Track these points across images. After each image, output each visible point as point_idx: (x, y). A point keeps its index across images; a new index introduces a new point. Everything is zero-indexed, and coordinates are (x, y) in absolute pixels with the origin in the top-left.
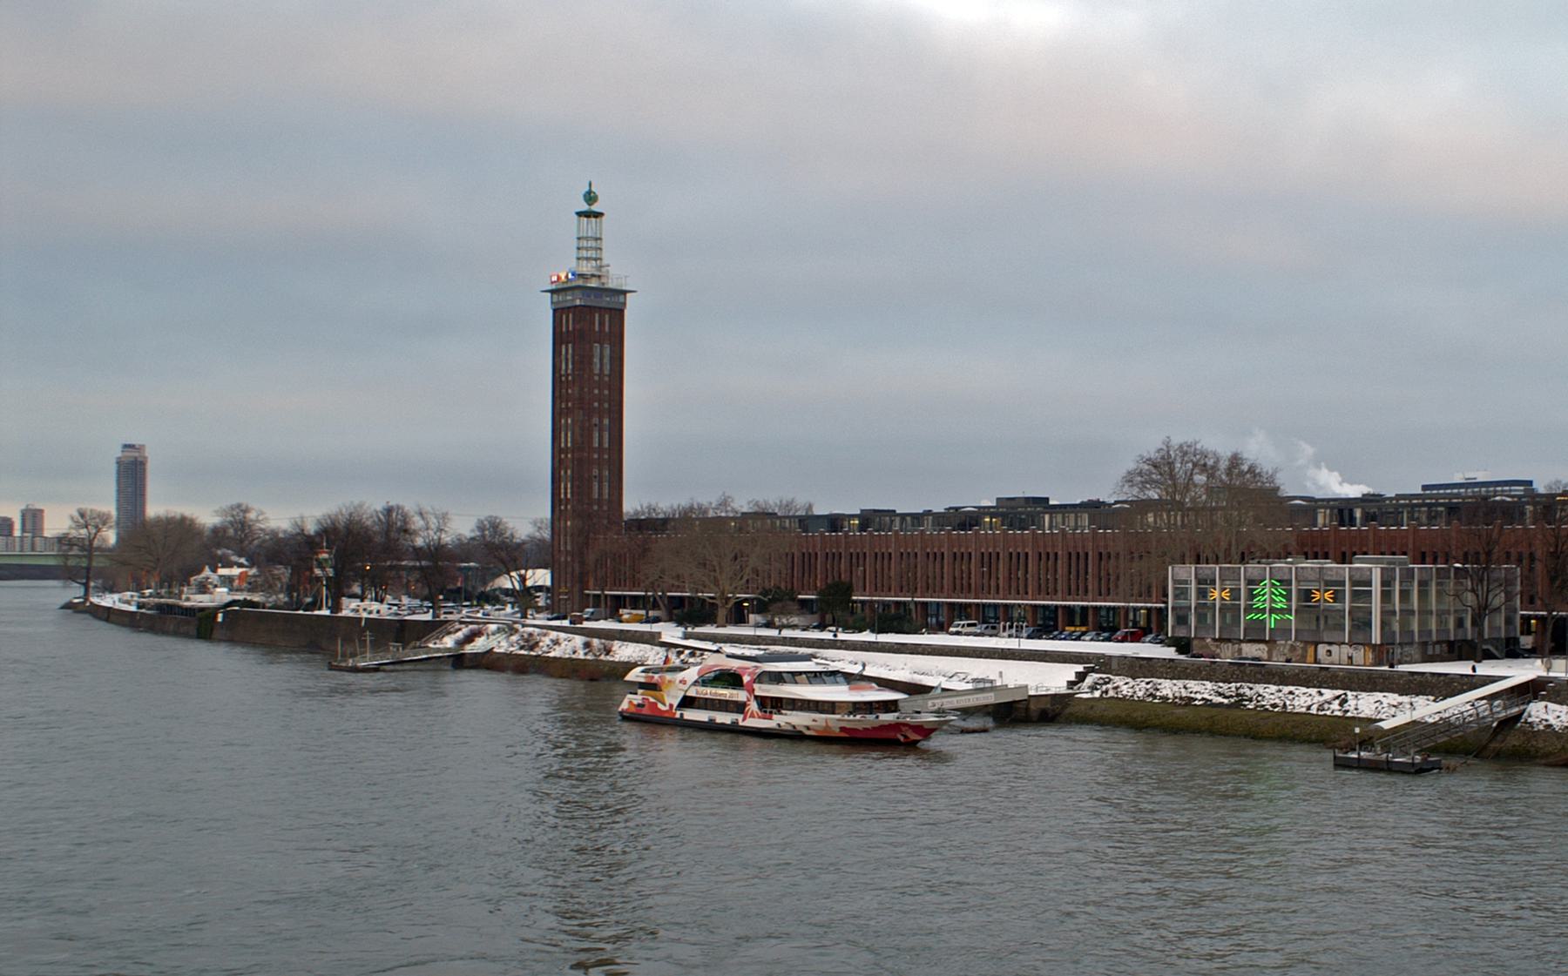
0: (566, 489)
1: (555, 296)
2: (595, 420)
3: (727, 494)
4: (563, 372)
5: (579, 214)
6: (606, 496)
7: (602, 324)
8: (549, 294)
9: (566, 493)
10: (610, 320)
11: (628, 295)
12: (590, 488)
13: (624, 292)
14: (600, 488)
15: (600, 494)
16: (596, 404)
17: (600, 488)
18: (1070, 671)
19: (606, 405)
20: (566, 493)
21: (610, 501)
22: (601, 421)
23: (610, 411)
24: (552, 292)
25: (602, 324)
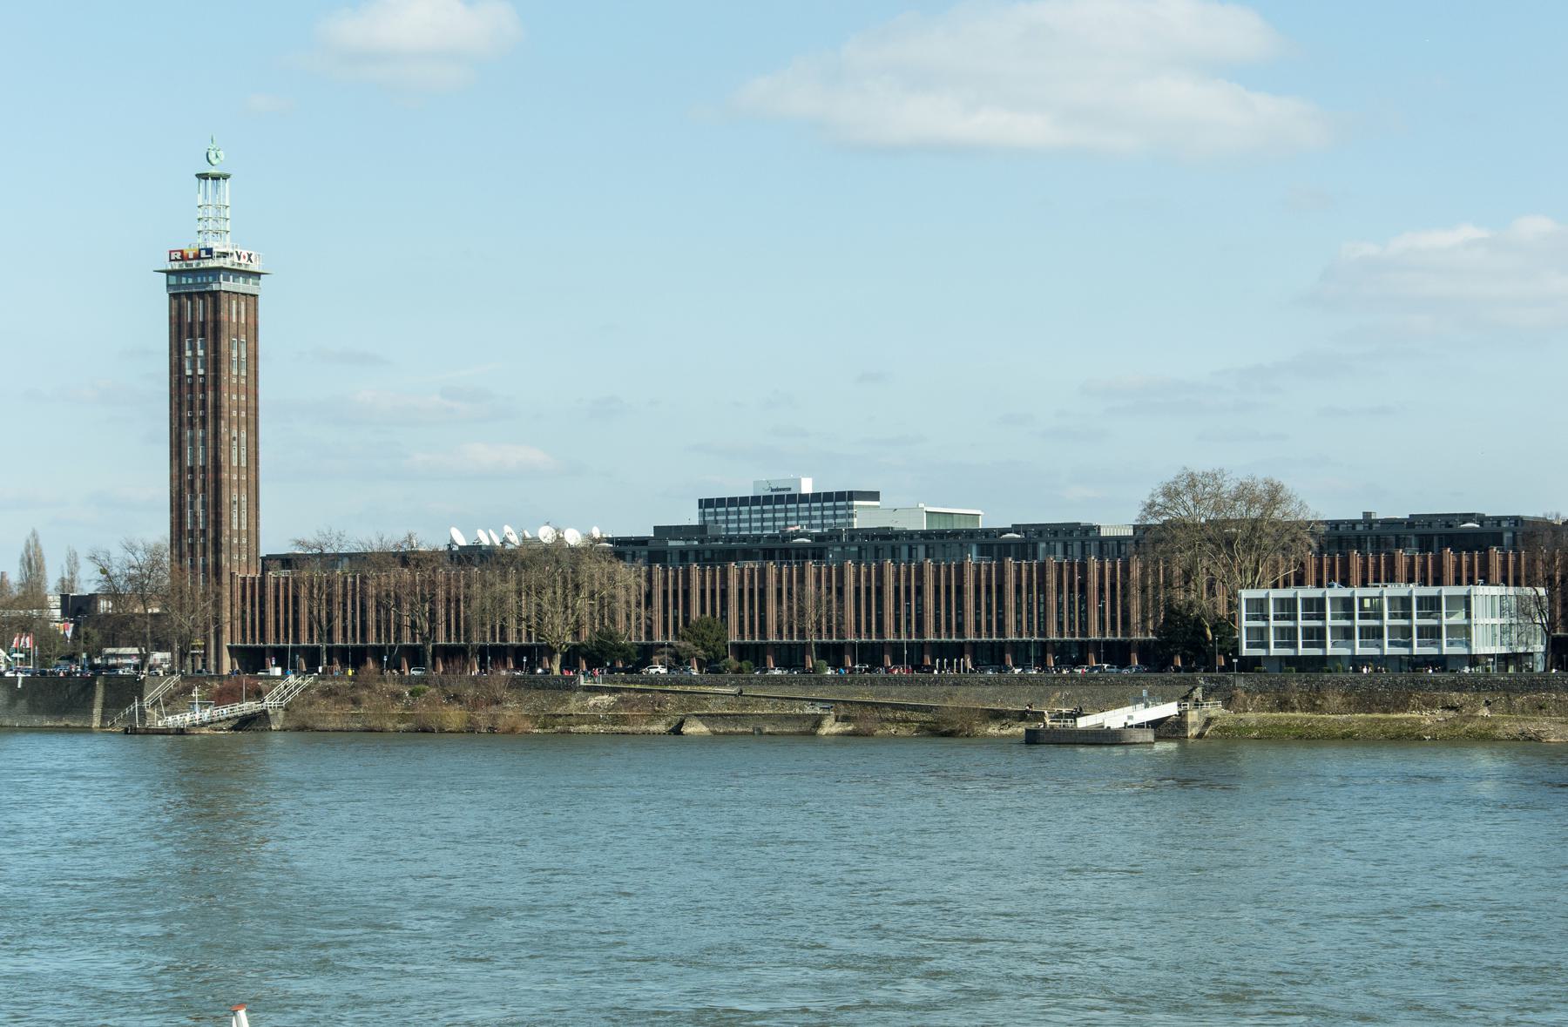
0: (194, 516)
4: (189, 372)
5: (199, 176)
11: (262, 276)
13: (258, 275)
16: (235, 413)
19: (243, 414)
20: (195, 523)
24: (169, 273)
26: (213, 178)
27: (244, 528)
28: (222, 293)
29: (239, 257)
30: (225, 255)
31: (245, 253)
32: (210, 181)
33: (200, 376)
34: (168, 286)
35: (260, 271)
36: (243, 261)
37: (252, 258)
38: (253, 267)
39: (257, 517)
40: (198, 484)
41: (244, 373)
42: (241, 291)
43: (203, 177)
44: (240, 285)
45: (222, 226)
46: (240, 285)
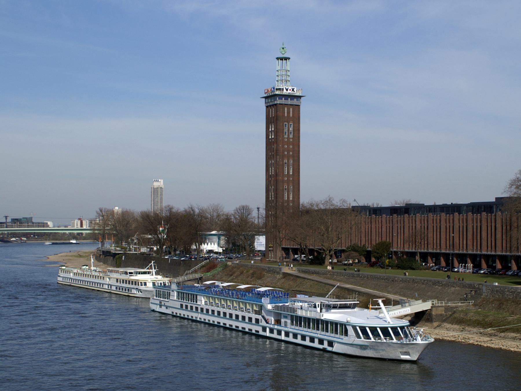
1: (267, 100)
2: (286, 161)
3: (330, 197)
5: (278, 59)
6: (291, 199)
7: (288, 113)
8: (264, 99)
9: (271, 198)
10: (293, 111)
12: (283, 195)
13: (300, 97)
14: (288, 195)
15: (288, 197)
16: (286, 153)
17: (288, 195)
18: (398, 299)
19: (291, 153)
20: (271, 198)
21: (293, 201)
22: (288, 161)
23: (293, 156)
24: (266, 98)
25: (288, 113)
26: (285, 60)
27: (291, 199)
28: (278, 105)
29: (287, 90)
30: (280, 89)
31: (290, 88)
32: (284, 61)
33: (291, 138)
34: (265, 103)
35: (301, 95)
36: (289, 91)
37: (295, 90)
38: (298, 94)
39: (299, 195)
40: (272, 182)
41: (291, 136)
42: (289, 103)
43: (278, 59)
44: (295, 102)
45: (288, 79)
46: (289, 102)
